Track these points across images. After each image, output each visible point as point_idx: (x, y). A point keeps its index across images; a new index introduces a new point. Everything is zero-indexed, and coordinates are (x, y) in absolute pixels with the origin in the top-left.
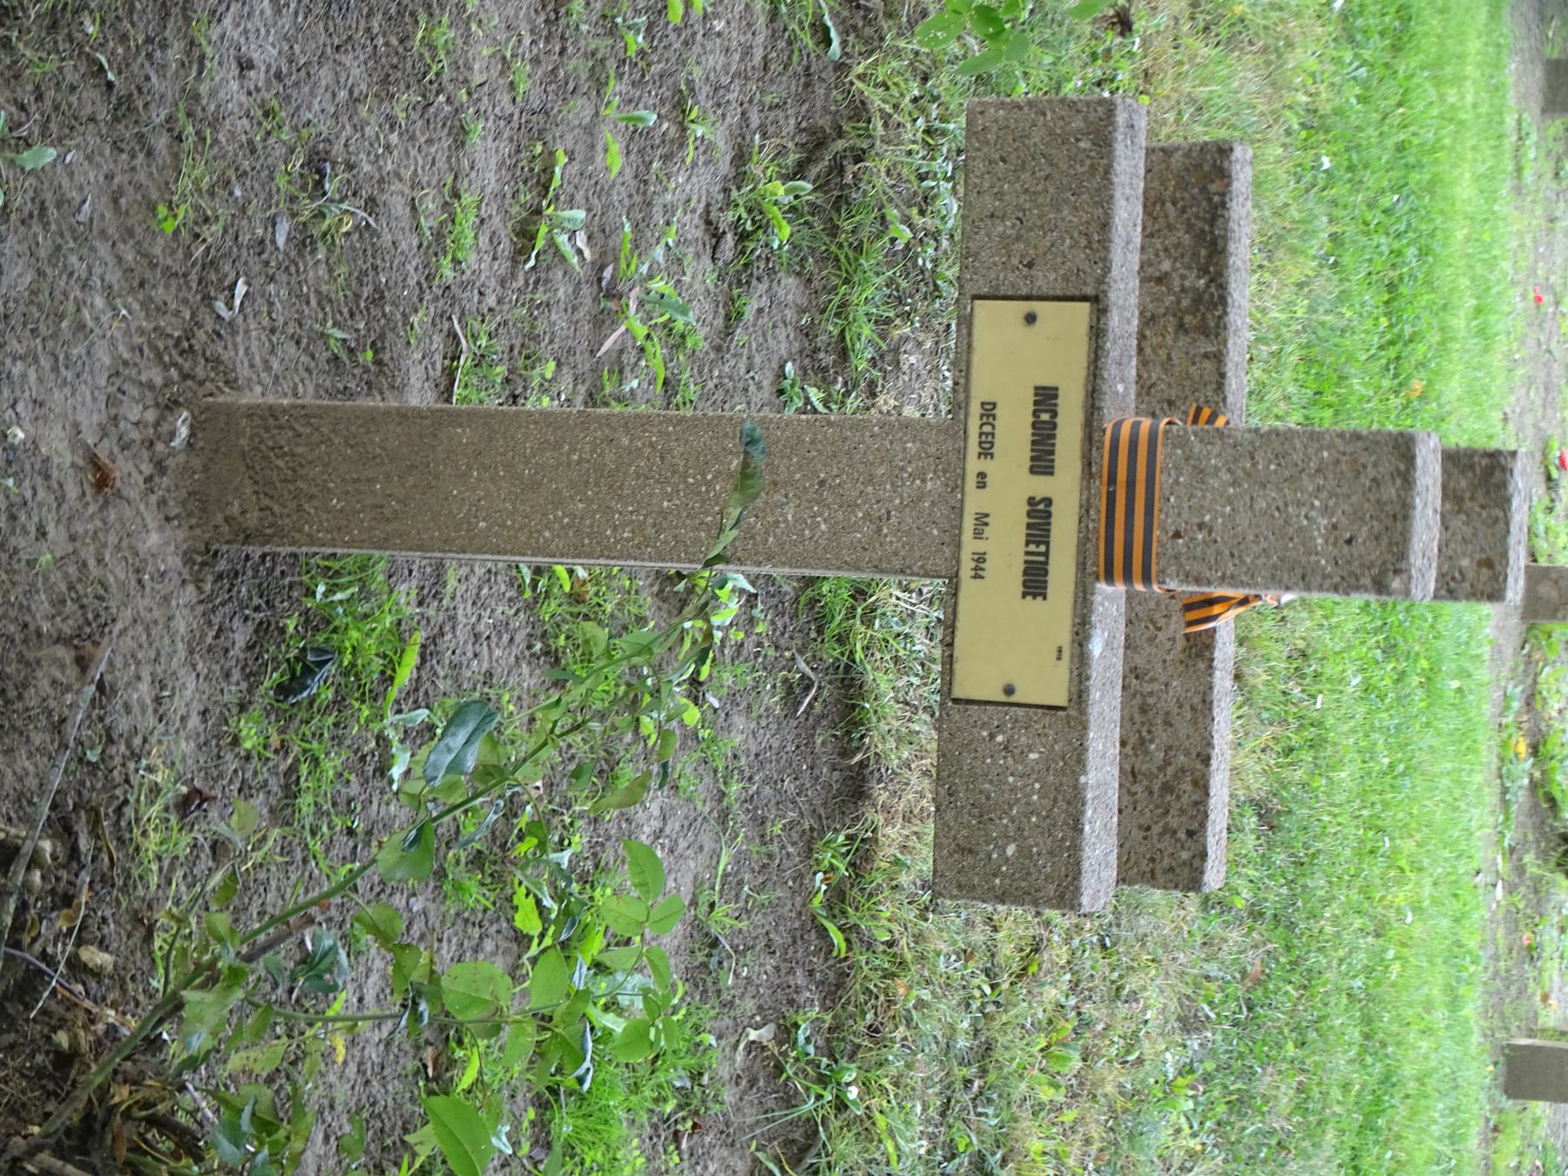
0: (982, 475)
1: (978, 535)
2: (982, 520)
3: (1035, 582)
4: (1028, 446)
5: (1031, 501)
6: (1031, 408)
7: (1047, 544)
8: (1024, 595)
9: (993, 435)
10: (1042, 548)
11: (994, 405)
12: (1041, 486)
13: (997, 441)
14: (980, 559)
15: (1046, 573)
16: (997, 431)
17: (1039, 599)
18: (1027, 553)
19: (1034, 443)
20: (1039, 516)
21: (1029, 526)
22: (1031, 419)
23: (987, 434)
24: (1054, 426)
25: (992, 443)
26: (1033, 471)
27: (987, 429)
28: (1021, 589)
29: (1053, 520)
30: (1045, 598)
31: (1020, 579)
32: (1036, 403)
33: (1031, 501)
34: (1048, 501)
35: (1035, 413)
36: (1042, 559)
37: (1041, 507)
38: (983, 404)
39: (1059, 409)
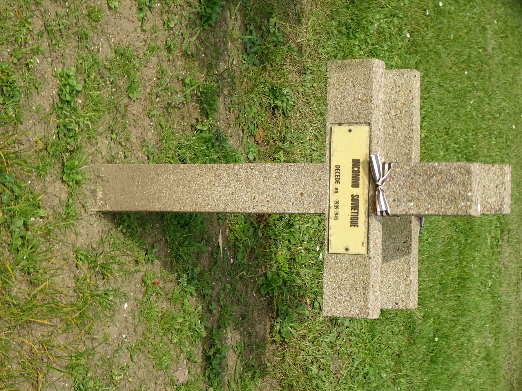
3: (354, 222)
4: (351, 178)
6: (352, 166)
7: (358, 210)
8: (351, 226)
10: (356, 211)
12: (355, 191)
14: (337, 214)
16: (341, 175)
19: (352, 177)
20: (355, 200)
21: (352, 204)
22: (352, 170)
23: (338, 176)
30: (357, 226)
31: (350, 221)
32: (353, 165)
33: (352, 196)
34: (358, 196)
35: (353, 168)
37: (356, 198)
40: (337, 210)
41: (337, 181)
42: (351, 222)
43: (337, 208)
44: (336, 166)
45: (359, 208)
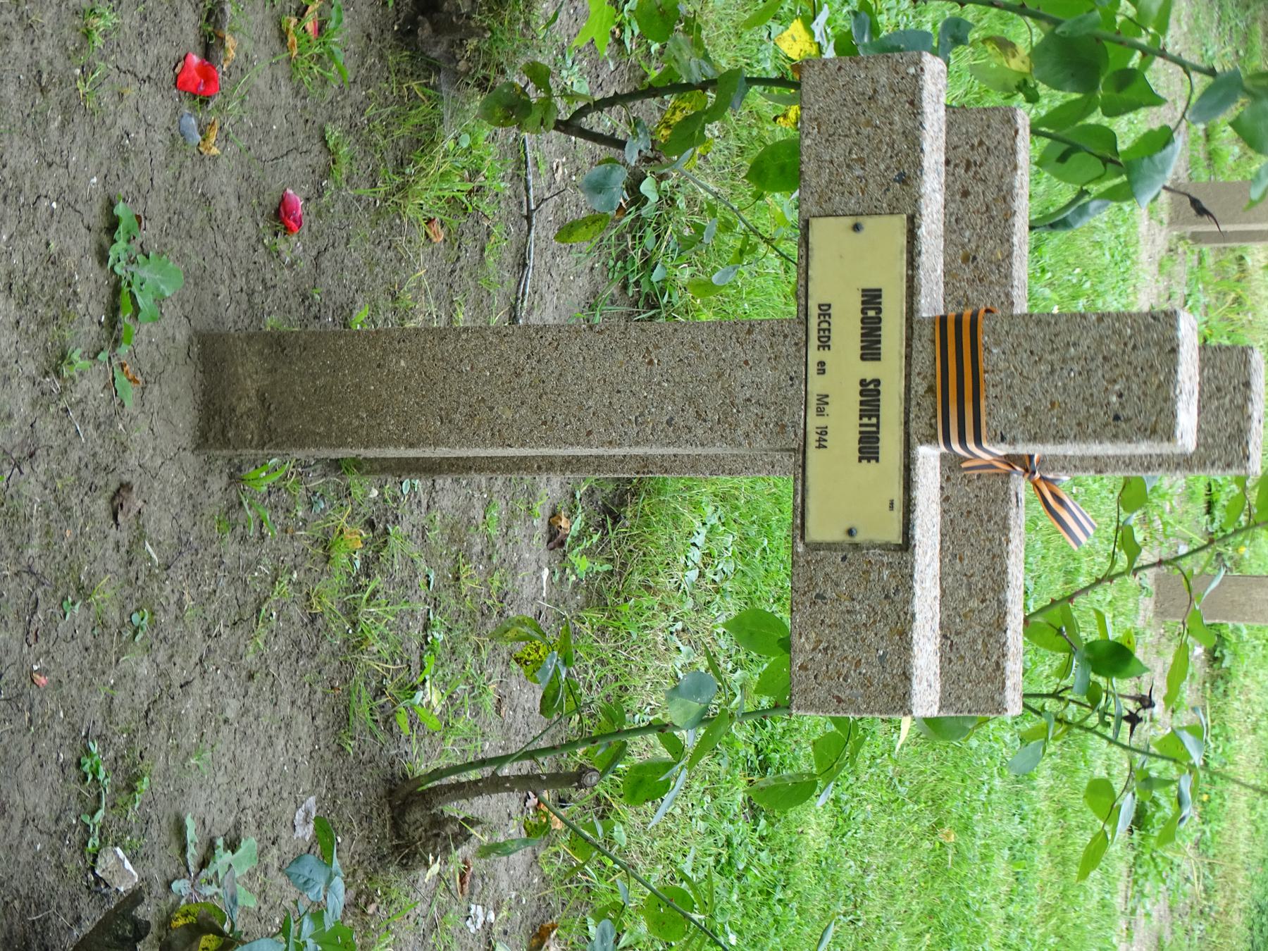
0: (822, 363)
1: (820, 412)
2: (823, 399)
3: (869, 448)
4: (859, 338)
6: (860, 306)
7: (878, 417)
8: (860, 460)
9: (829, 330)
10: (874, 420)
11: (829, 306)
12: (870, 370)
13: (832, 335)
15: (878, 439)
17: (873, 462)
18: (861, 425)
20: (870, 394)
21: (862, 403)
22: (861, 316)
23: (824, 330)
24: (880, 320)
25: (829, 338)
26: (863, 358)
27: (824, 325)
28: (858, 454)
29: (882, 397)
31: (856, 446)
32: (863, 303)
34: (877, 382)
35: (863, 311)
36: (874, 429)
37: (872, 387)
38: (820, 306)
41: (824, 344)
42: (860, 450)
44: (820, 306)
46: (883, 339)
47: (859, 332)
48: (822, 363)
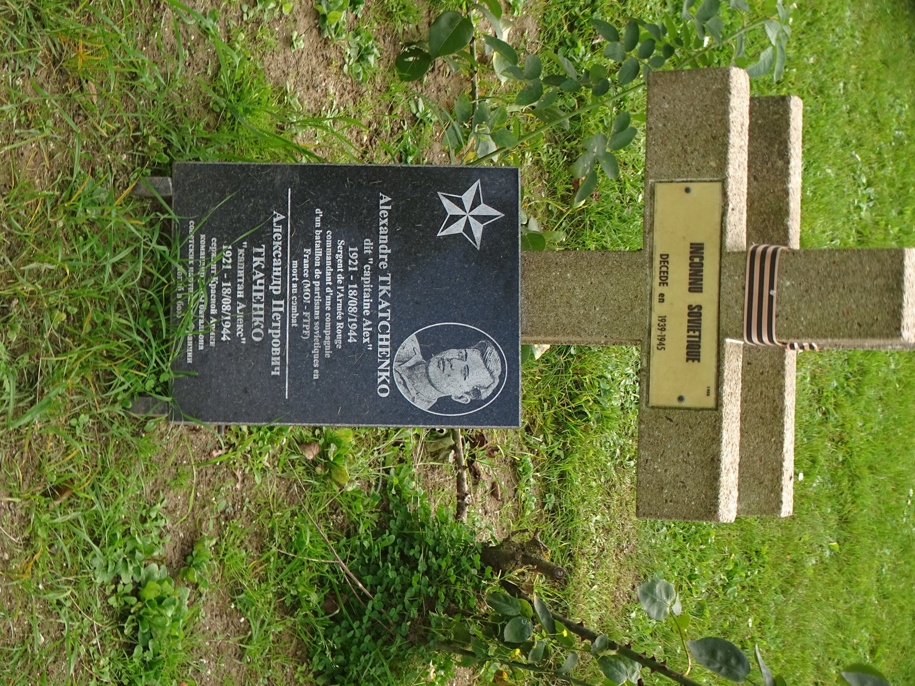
0: (662, 295)
3: (693, 352)
4: (688, 277)
5: (690, 307)
6: (689, 255)
7: (700, 331)
8: (687, 360)
10: (697, 333)
11: (668, 255)
12: (695, 299)
13: (670, 276)
14: (662, 339)
15: (699, 347)
17: (696, 362)
18: (689, 337)
19: (690, 275)
20: (695, 315)
21: (689, 321)
22: (689, 261)
23: (664, 272)
24: (702, 265)
26: (690, 290)
28: (686, 356)
29: (703, 317)
31: (685, 351)
32: (691, 252)
33: (690, 307)
34: (700, 307)
35: (691, 258)
38: (661, 255)
39: (704, 256)
40: (664, 333)
41: (664, 282)
42: (687, 354)
43: (663, 329)
44: (661, 255)
45: (703, 328)
46: (704, 278)
47: (688, 272)
48: (662, 295)
